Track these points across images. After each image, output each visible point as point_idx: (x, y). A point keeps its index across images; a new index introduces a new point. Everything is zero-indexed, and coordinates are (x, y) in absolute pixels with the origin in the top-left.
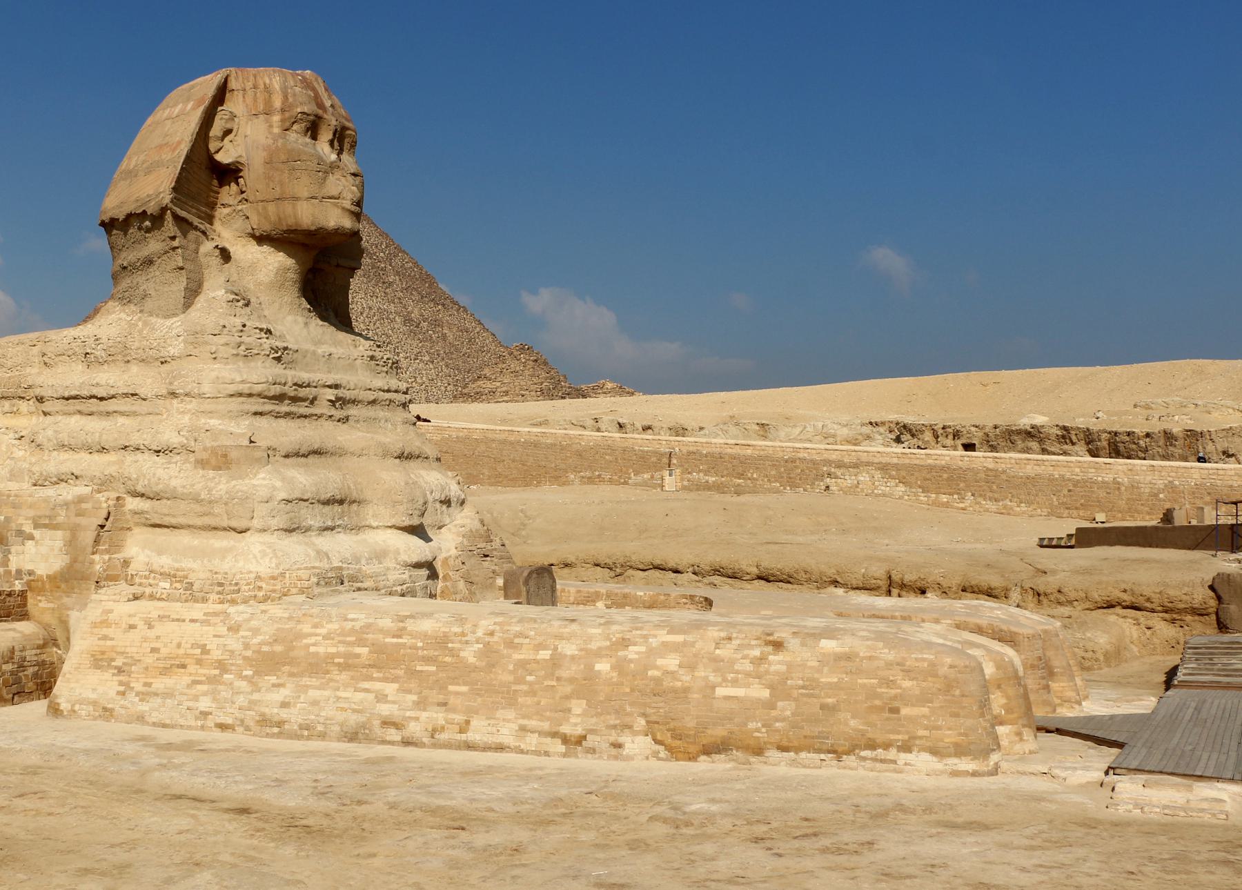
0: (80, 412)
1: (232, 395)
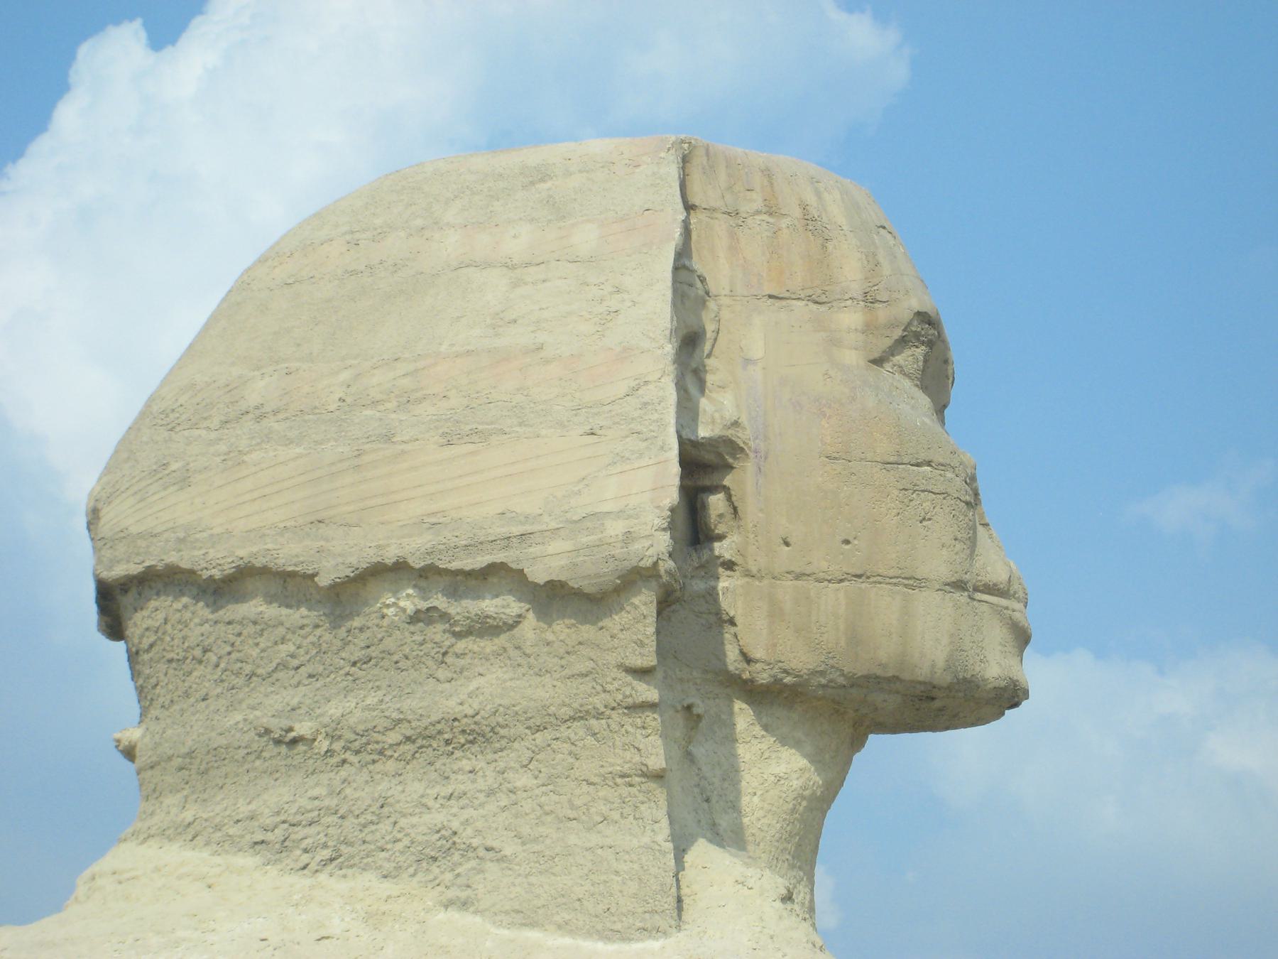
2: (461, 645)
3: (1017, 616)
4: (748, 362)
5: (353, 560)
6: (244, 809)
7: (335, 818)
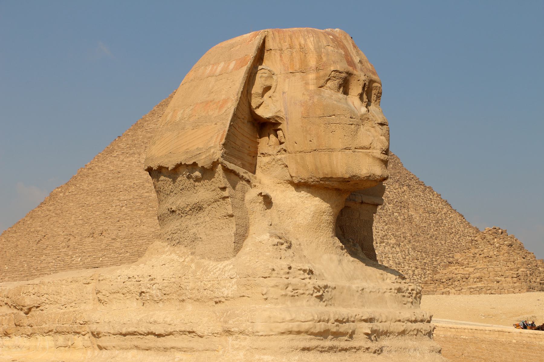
0: (137, 347)
1: (283, 333)
2: (196, 184)
3: (375, 154)
4: (284, 93)
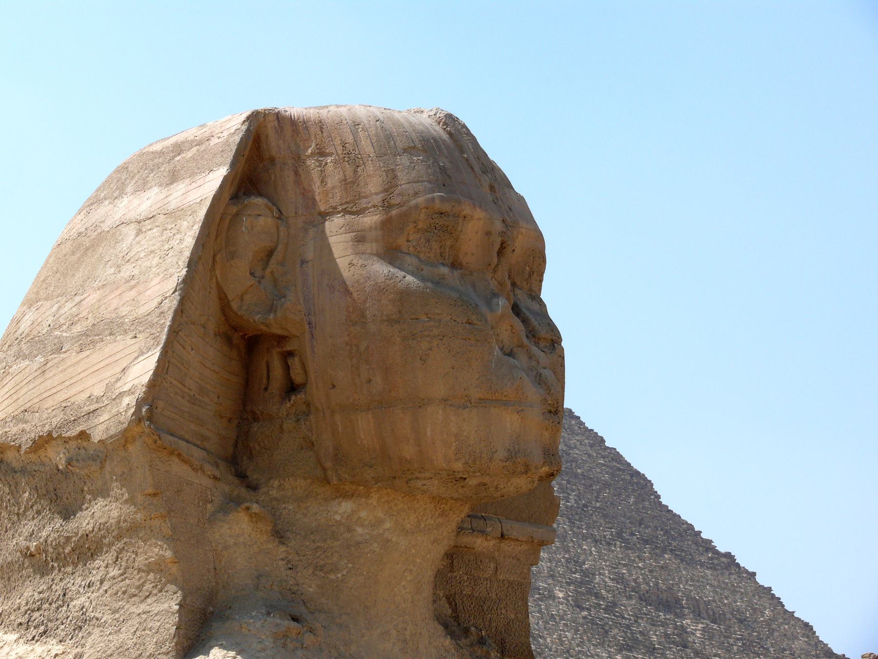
4: (303, 262)
5: (33, 435)
6: (18, 601)
7: (46, 606)
